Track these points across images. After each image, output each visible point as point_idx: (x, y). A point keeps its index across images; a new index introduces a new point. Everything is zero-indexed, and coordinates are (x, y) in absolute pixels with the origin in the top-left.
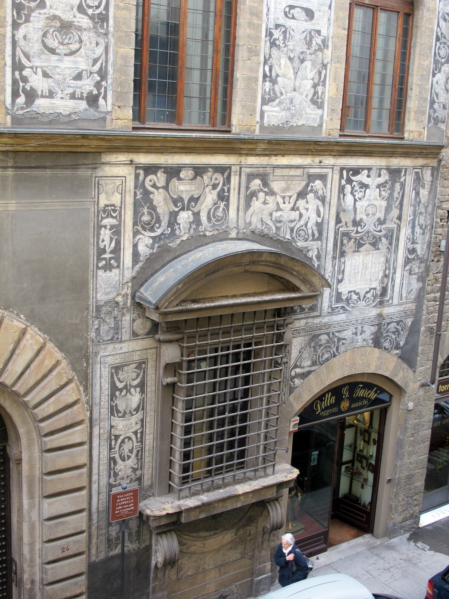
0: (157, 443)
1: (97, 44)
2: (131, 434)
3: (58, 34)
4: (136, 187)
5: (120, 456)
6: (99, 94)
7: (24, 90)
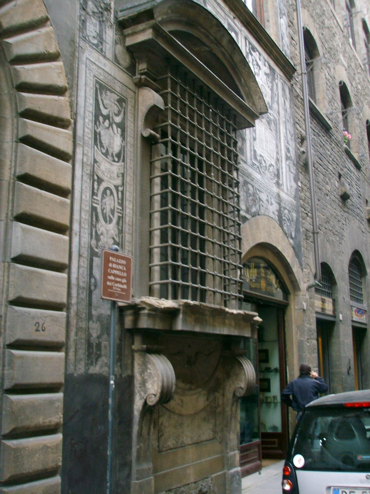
0: (136, 218)
2: (113, 186)
5: (102, 210)
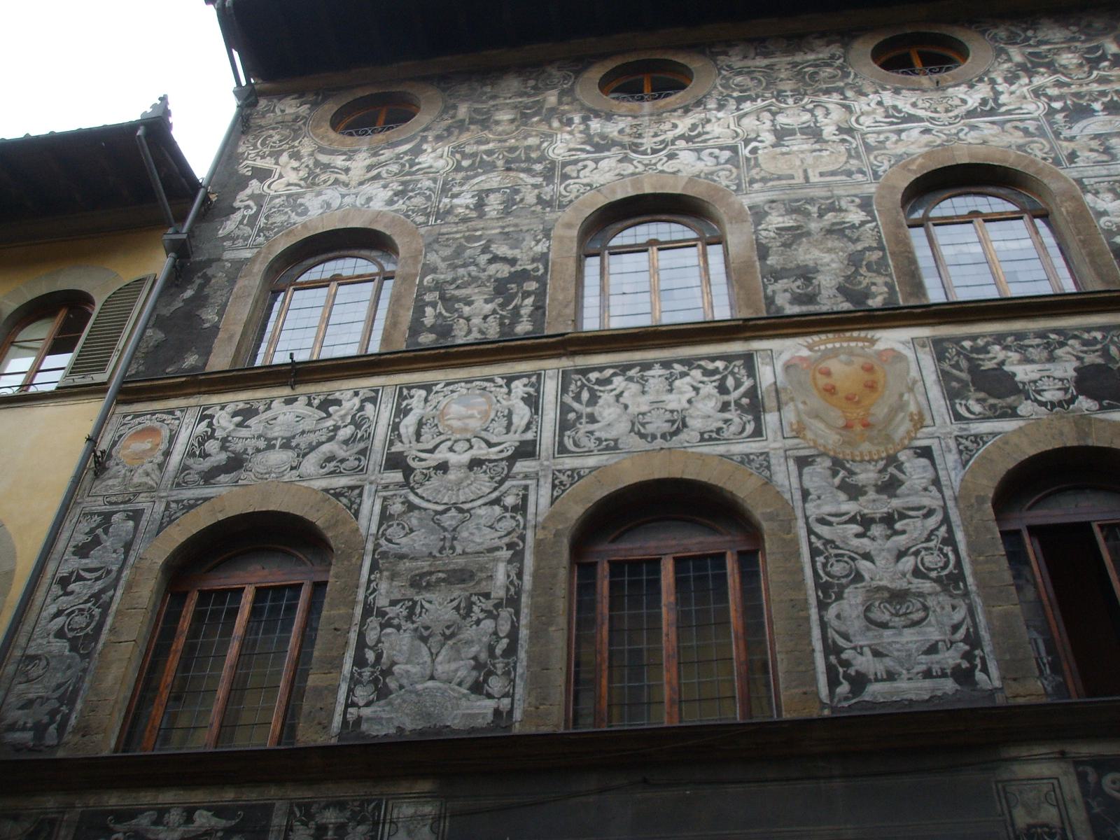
1: (954, 608)
3: (888, 606)
4: (1085, 793)
6: (973, 667)
7: (847, 676)
